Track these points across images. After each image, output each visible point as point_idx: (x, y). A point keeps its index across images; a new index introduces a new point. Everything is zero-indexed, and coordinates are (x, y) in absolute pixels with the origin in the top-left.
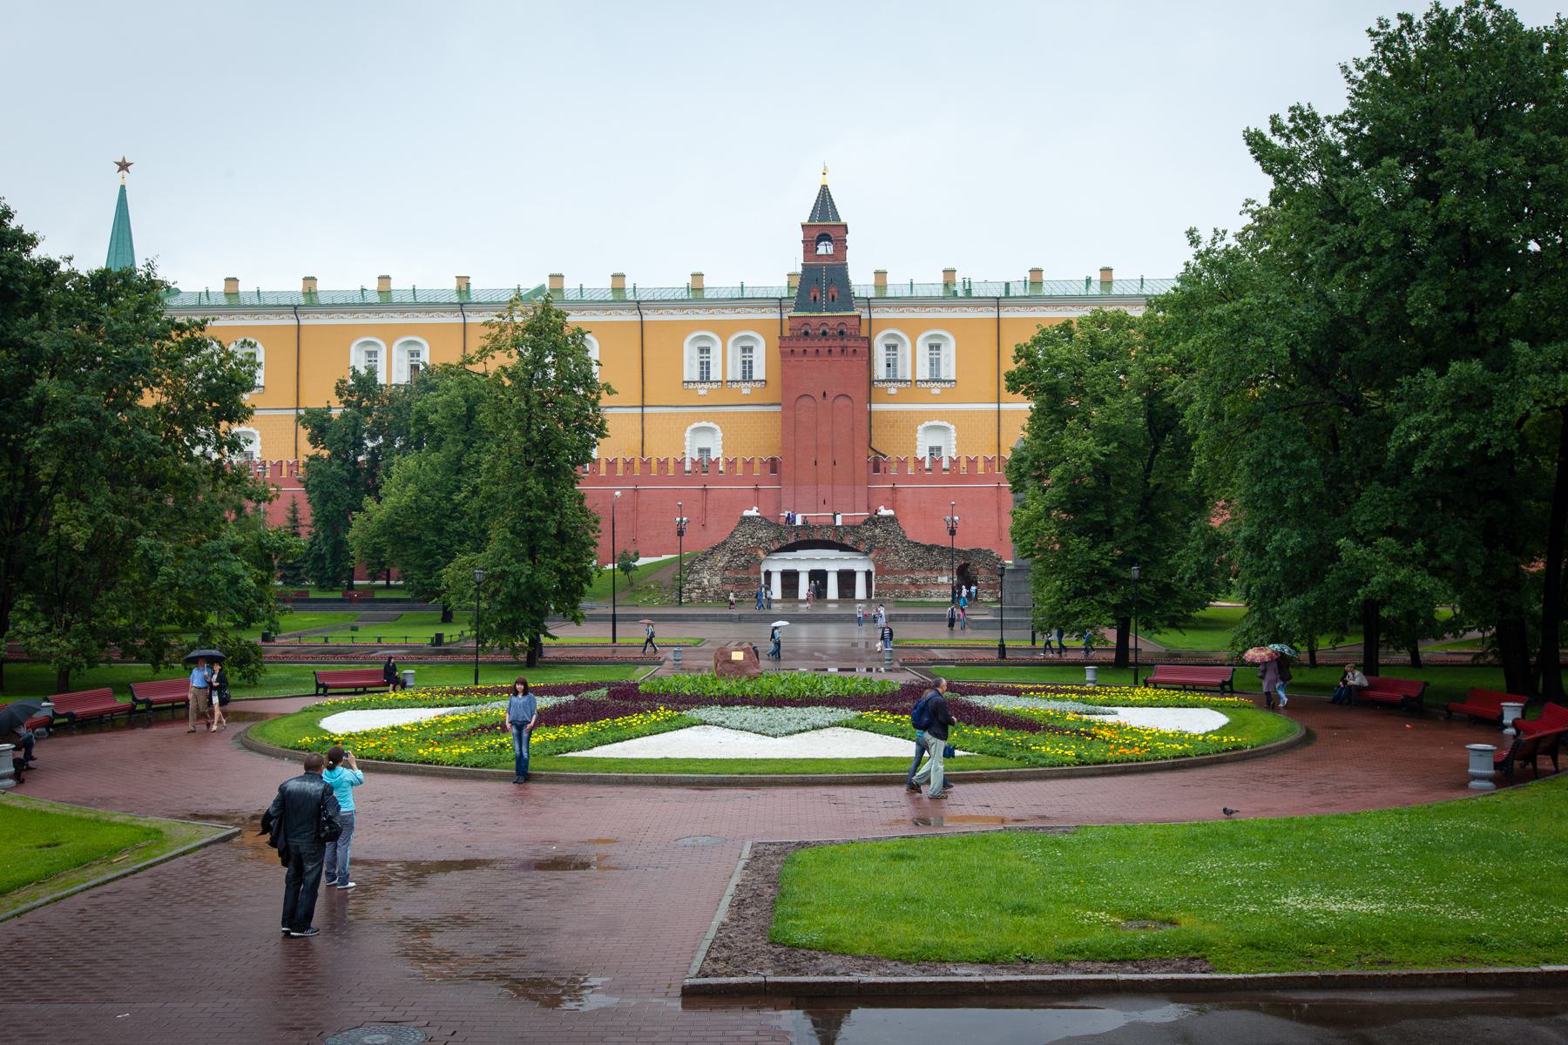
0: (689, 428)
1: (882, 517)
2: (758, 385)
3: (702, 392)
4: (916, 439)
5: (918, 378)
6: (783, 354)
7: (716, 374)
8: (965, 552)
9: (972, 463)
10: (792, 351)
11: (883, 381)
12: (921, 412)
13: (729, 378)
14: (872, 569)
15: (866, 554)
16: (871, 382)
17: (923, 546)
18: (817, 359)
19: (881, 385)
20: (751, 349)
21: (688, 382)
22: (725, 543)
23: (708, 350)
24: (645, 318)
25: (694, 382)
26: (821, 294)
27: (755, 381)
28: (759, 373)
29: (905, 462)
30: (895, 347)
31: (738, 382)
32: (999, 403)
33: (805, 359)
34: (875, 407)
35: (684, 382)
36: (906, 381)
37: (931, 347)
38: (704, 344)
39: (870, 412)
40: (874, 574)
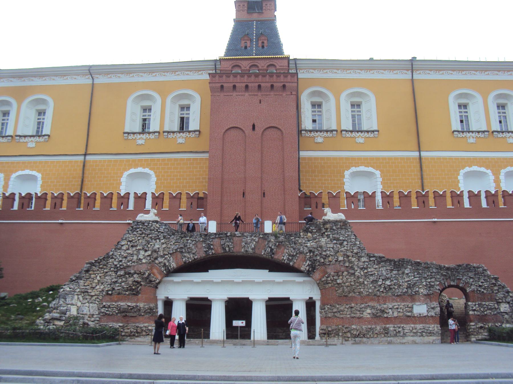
0: (126, 174)
1: (325, 223)
2: (192, 135)
3: (140, 142)
4: (344, 184)
5: (343, 128)
6: (212, 90)
7: (154, 126)
8: (448, 269)
9: (404, 198)
10: (222, 87)
11: (310, 131)
12: (347, 159)
13: (166, 129)
14: (316, 295)
15: (308, 274)
16: (300, 132)
17: (390, 261)
18: (247, 94)
19: (308, 134)
20: (188, 108)
21: (128, 133)
22: (108, 257)
23: (150, 110)
24: (96, 81)
25: (134, 133)
26: (251, 40)
27: (190, 132)
28: (194, 125)
29: (337, 197)
30: (320, 105)
31: (174, 132)
32: (420, 151)
33: (235, 94)
34: (303, 154)
35: (125, 133)
36: (332, 131)
37: (353, 106)
38: (146, 103)
39: (299, 158)
40: (318, 305)
